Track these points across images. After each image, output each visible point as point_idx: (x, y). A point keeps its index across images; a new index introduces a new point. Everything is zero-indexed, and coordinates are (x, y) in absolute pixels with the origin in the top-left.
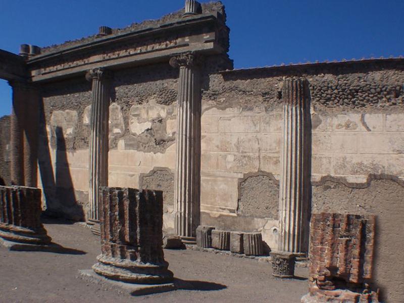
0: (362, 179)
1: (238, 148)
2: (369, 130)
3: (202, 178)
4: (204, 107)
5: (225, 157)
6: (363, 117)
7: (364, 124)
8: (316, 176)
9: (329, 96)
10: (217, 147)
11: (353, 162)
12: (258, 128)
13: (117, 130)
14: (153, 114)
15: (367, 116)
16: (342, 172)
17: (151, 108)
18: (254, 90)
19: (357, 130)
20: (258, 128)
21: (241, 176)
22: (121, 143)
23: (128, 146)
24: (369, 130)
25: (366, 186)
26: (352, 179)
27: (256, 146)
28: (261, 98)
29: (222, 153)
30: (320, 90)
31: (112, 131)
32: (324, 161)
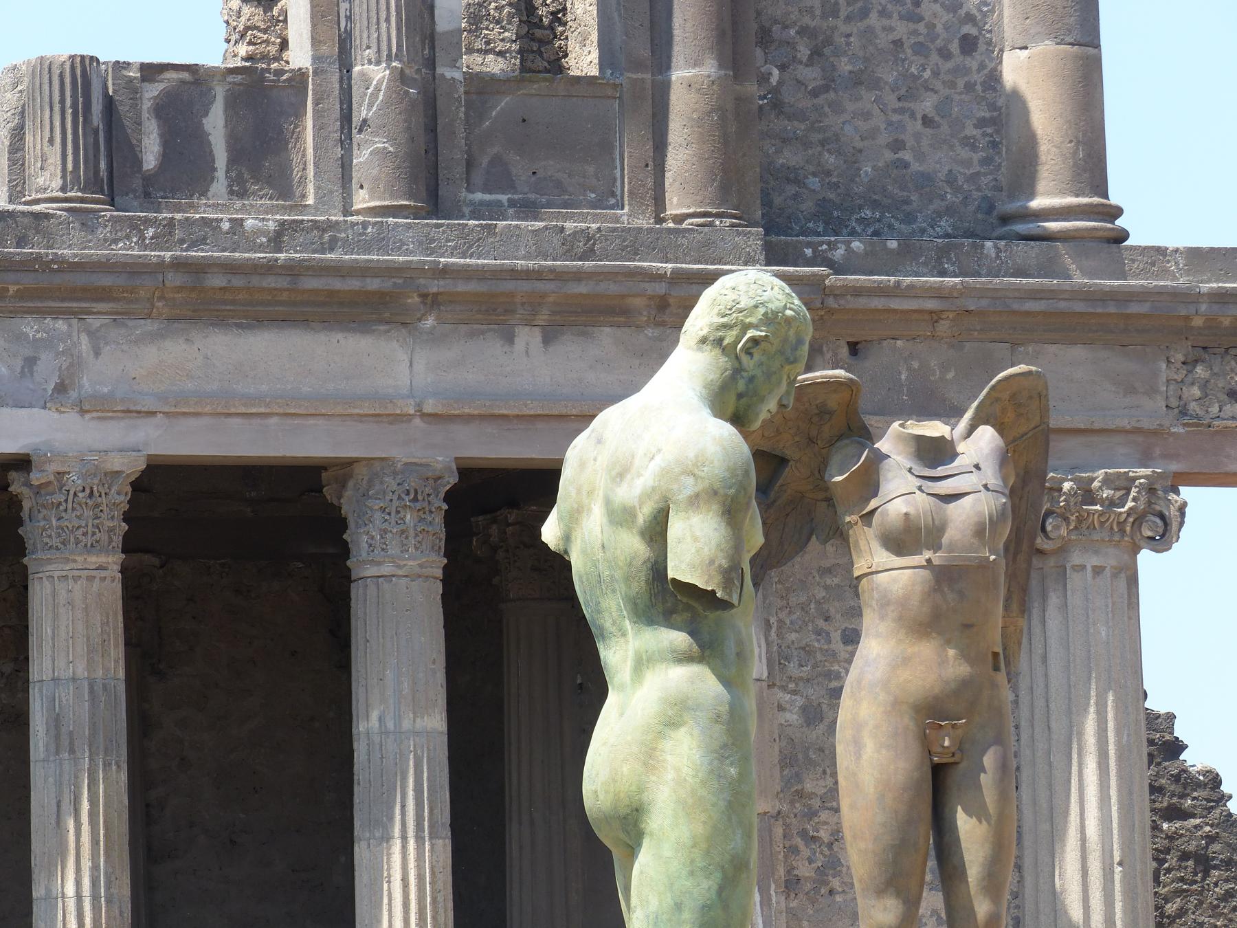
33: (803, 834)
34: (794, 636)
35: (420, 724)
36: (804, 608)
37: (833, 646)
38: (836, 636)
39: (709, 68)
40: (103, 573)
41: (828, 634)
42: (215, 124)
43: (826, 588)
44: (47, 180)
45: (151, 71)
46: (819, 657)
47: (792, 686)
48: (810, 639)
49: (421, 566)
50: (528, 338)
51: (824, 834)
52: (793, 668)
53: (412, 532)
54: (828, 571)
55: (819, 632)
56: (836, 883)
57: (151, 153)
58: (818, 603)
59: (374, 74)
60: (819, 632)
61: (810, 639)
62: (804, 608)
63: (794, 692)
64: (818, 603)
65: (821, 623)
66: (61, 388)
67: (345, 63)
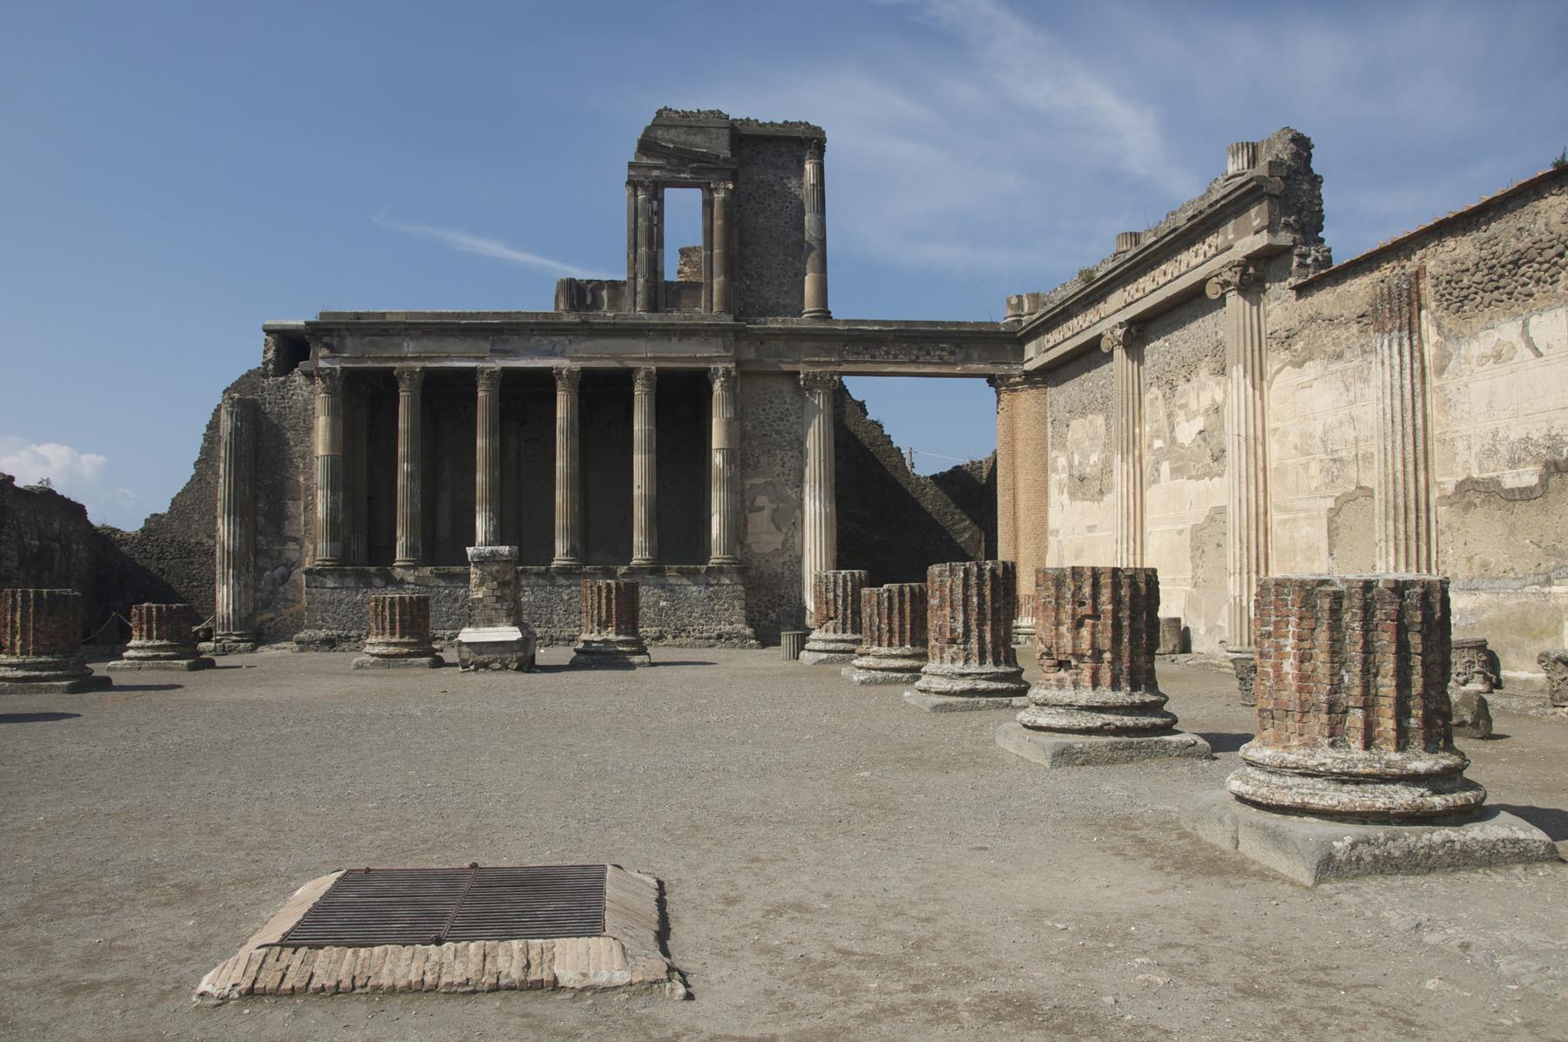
0: (1529, 476)
1: (1324, 443)
2: (1539, 354)
3: (1275, 517)
4: (1271, 367)
5: (1306, 467)
6: (1525, 324)
7: (1529, 343)
8: (1445, 480)
9: (1464, 292)
10: (1296, 448)
11: (1511, 438)
12: (1351, 394)
13: (1158, 443)
14: (1205, 400)
15: (1534, 320)
16: (1492, 466)
17: (1203, 387)
18: (1345, 313)
19: (1516, 359)
20: (1351, 396)
21: (1330, 503)
22: (1165, 467)
23: (1176, 472)
24: (1539, 354)
25: (1539, 492)
26: (1510, 481)
27: (1351, 434)
28: (1355, 328)
29: (1303, 460)
30: (1448, 282)
31: (1150, 446)
32: (1460, 445)
39: (722, 278)
42: (605, 293)
44: (562, 306)
45: (589, 282)
50: (675, 340)
57: (589, 300)
59: (641, 280)
67: (635, 278)
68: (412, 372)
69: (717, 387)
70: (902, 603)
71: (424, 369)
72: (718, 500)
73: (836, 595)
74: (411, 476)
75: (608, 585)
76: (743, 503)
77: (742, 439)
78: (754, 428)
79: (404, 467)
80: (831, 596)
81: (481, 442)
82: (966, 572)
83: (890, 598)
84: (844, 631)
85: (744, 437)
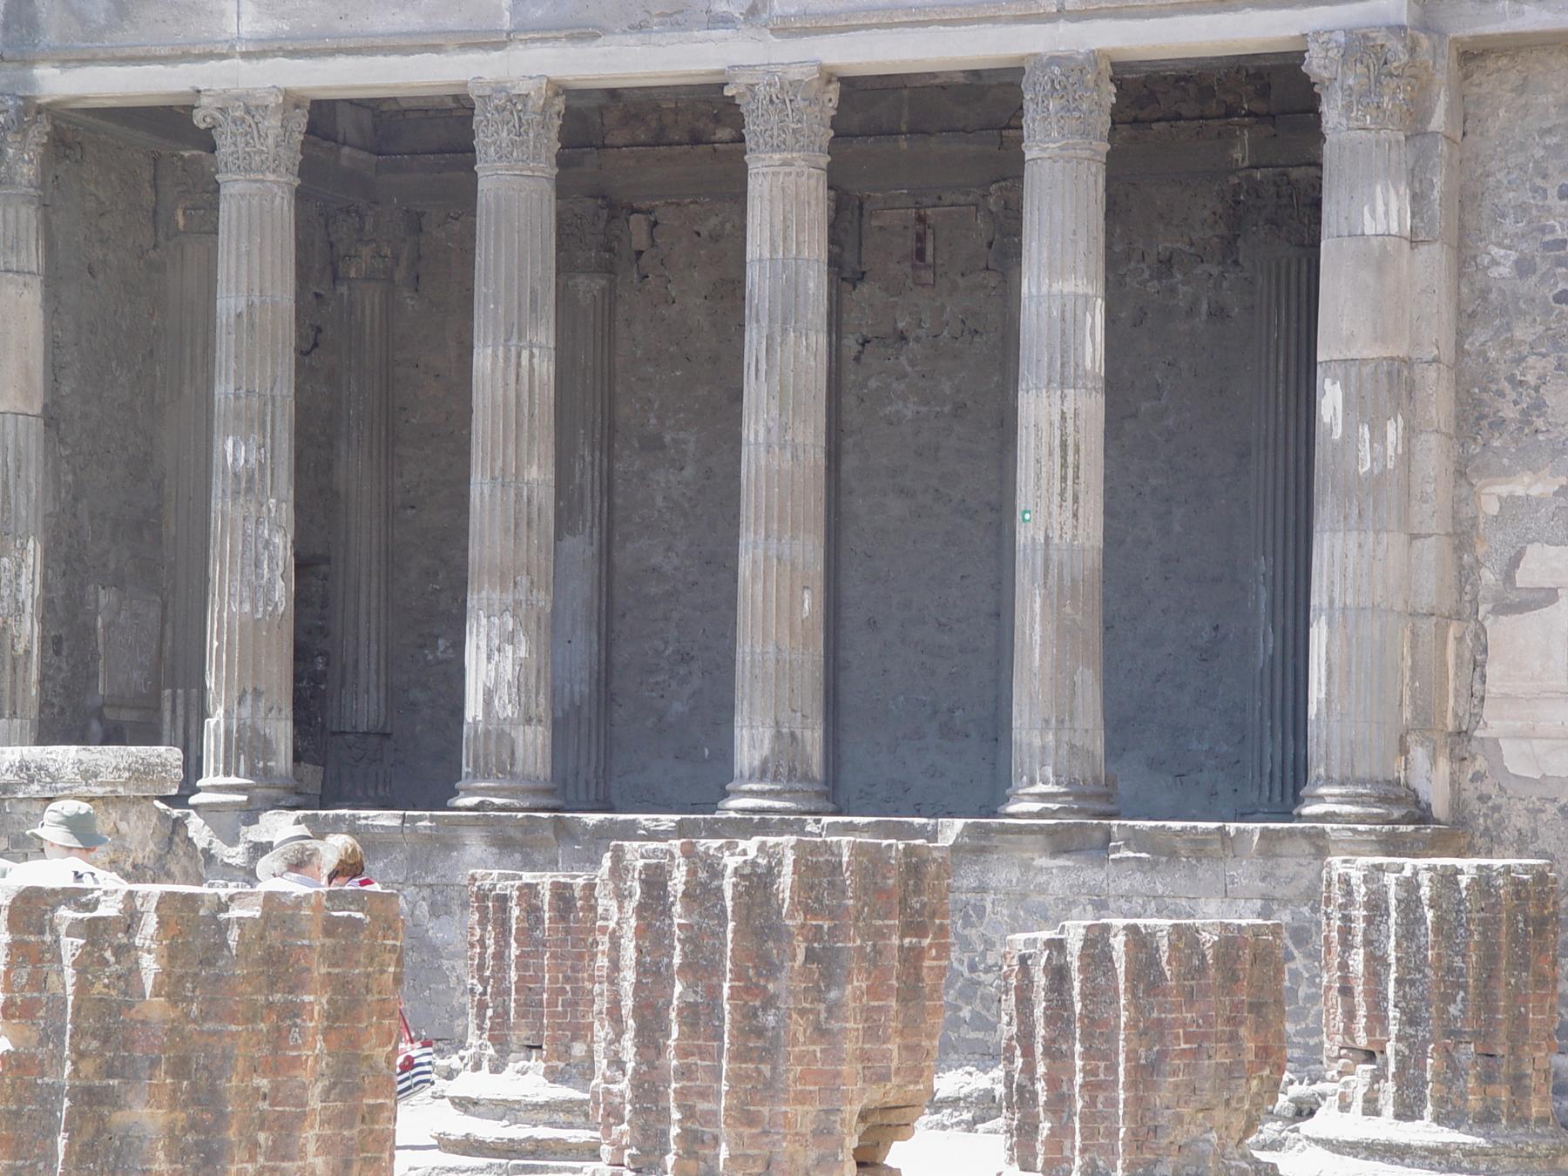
33: (1511, 379)
34: (1511, 194)
35: (1056, 288)
36: (1522, 168)
37: (1548, 202)
38: (1553, 192)
40: (788, 169)
41: (1545, 191)
43: (1546, 147)
46: (1534, 212)
47: (1507, 242)
48: (1528, 198)
49: (1061, 148)
51: (1531, 379)
52: (1509, 224)
53: (1054, 120)
54: (1549, 131)
55: (1535, 190)
56: (1540, 423)
58: (1536, 162)
60: (1535, 190)
61: (1528, 198)
62: (1522, 168)
63: (1510, 248)
64: (1536, 162)
65: (1539, 182)
66: (753, 11)
68: (253, 109)
69: (1332, 114)
70: (1097, 994)
71: (291, 100)
72: (1339, 559)
73: (1375, 962)
74: (248, 484)
75: (530, 891)
76: (1465, 576)
77: (1465, 319)
78: (1524, 267)
79: (232, 452)
80: (1357, 961)
81: (484, 360)
82: (655, 881)
83: (1058, 975)
84: (1407, 1111)
85: (1473, 308)
